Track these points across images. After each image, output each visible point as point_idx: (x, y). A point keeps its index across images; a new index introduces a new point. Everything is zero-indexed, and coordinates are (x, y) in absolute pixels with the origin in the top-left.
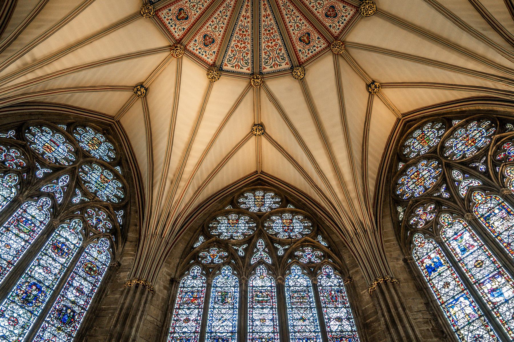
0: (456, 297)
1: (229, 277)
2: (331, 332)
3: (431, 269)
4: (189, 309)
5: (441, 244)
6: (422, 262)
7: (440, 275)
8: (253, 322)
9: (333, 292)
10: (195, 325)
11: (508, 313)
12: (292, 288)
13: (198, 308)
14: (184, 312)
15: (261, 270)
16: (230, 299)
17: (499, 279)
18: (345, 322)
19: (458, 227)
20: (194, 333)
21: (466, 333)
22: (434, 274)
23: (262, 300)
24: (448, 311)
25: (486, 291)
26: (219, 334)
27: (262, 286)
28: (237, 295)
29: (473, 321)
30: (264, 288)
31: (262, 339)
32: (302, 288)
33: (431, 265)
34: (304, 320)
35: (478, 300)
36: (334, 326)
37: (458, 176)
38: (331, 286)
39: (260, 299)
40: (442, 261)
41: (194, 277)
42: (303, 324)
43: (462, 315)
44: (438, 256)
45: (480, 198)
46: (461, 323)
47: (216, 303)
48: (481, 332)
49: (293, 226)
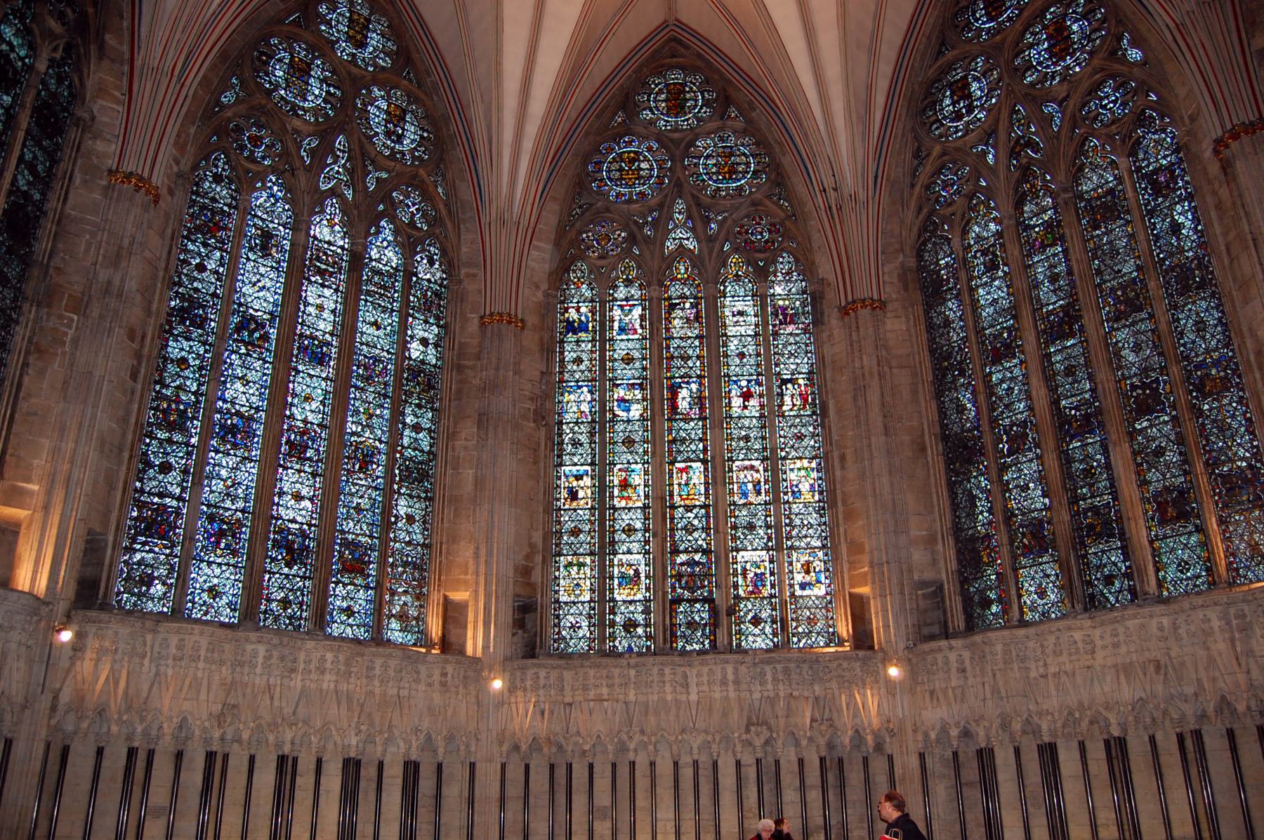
0: (580, 384)
1: (277, 201)
2: (410, 358)
3: (571, 327)
4: (205, 245)
5: (603, 303)
6: (566, 310)
7: (577, 342)
8: (305, 306)
9: (429, 294)
10: (213, 280)
11: (621, 434)
12: (374, 263)
13: (221, 249)
14: (196, 249)
15: (332, 207)
16: (274, 250)
17: (637, 392)
18: (431, 350)
19: (635, 292)
20: (214, 295)
21: (568, 431)
22: (571, 337)
23: (326, 270)
24: (562, 395)
25: (616, 397)
26: (251, 311)
27: (329, 243)
28: (287, 245)
29: (582, 423)
30: (331, 248)
31: (314, 339)
32: (388, 268)
33: (574, 321)
34: (378, 328)
35: (603, 403)
36: (415, 350)
37: (680, 213)
38: (429, 281)
39: (324, 267)
40: (590, 325)
41: (218, 179)
42: (376, 333)
43: (575, 409)
44: (590, 315)
45: (683, 271)
46: (568, 417)
47: (251, 249)
48: (584, 439)
49: (403, 129)
